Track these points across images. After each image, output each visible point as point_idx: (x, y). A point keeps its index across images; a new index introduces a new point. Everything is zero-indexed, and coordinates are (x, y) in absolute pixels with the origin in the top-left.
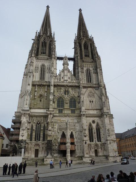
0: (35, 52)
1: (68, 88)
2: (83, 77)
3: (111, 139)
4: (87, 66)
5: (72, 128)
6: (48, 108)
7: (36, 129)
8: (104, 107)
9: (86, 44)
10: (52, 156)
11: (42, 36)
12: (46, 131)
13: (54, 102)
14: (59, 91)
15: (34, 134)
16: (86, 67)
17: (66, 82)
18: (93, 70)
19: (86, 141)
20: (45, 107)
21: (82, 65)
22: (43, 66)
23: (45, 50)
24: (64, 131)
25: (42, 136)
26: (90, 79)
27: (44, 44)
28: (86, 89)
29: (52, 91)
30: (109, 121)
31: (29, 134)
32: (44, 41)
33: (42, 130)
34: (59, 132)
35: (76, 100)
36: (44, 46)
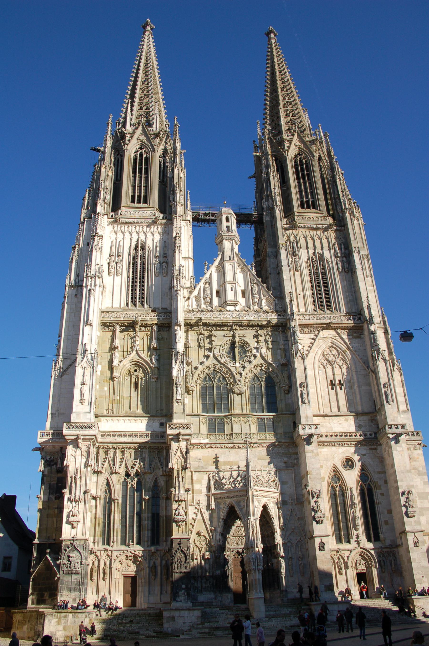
0: (108, 197)
1: (242, 333)
2: (299, 288)
3: (419, 528)
5: (270, 490)
6: (164, 412)
8: (387, 402)
9: (301, 161)
10: (195, 603)
11: (132, 135)
13: (188, 391)
15: (117, 517)
19: (324, 540)
21: (292, 239)
22: (140, 248)
26: (327, 293)
27: (141, 164)
28: (312, 336)
29: (180, 347)
30: (407, 460)
32: (141, 155)
35: (276, 380)
36: (140, 172)
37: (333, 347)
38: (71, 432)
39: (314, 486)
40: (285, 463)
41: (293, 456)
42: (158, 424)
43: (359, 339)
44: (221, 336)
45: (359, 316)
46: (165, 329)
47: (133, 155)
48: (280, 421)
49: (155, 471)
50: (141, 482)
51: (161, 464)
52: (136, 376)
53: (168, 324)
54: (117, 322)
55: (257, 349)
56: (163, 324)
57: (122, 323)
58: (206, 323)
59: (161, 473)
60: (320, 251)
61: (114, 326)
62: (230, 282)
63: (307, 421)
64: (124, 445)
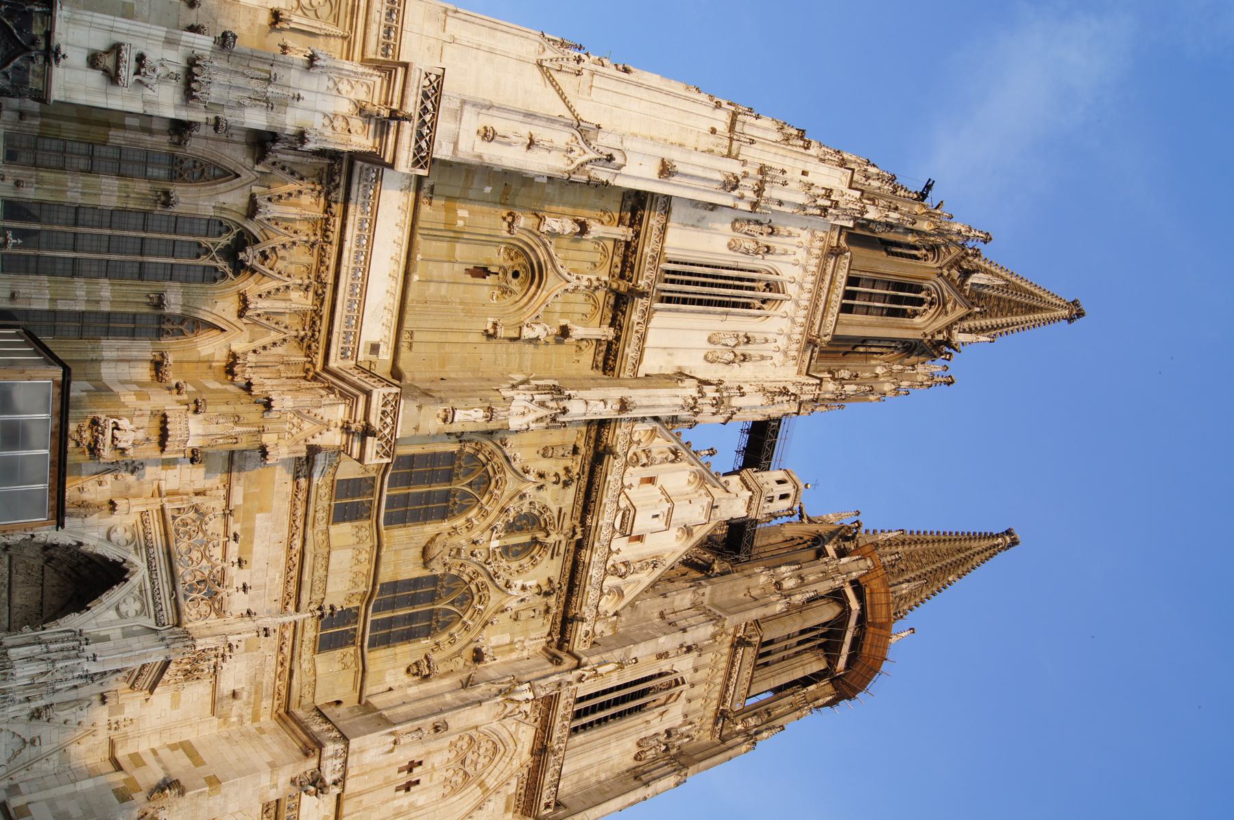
4: (702, 674)
7: (176, 224)
12: (144, 349)
14: (546, 465)
16: (696, 670)
17: (617, 526)
18: (668, 733)
20: (407, 325)
22: (768, 295)
23: (867, 311)
24: (139, 576)
25: (81, 307)
31: (109, 125)
33: (159, 303)
34: (121, 504)
35: (443, 638)
37: (494, 754)
38: (415, 90)
39: (176, 808)
40: (234, 695)
41: (250, 711)
42: (375, 339)
43: (503, 811)
44: (563, 500)
45: (553, 805)
46: (600, 358)
47: (926, 284)
48: (346, 667)
49: (244, 328)
50: (215, 280)
51: (265, 348)
52: (505, 273)
53: (613, 369)
54: (642, 235)
55: (524, 588)
56: (616, 356)
57: (636, 248)
58: (601, 463)
59: (238, 347)
60: (684, 695)
61: (631, 225)
62: (670, 512)
63: (353, 754)
64: (334, 237)
